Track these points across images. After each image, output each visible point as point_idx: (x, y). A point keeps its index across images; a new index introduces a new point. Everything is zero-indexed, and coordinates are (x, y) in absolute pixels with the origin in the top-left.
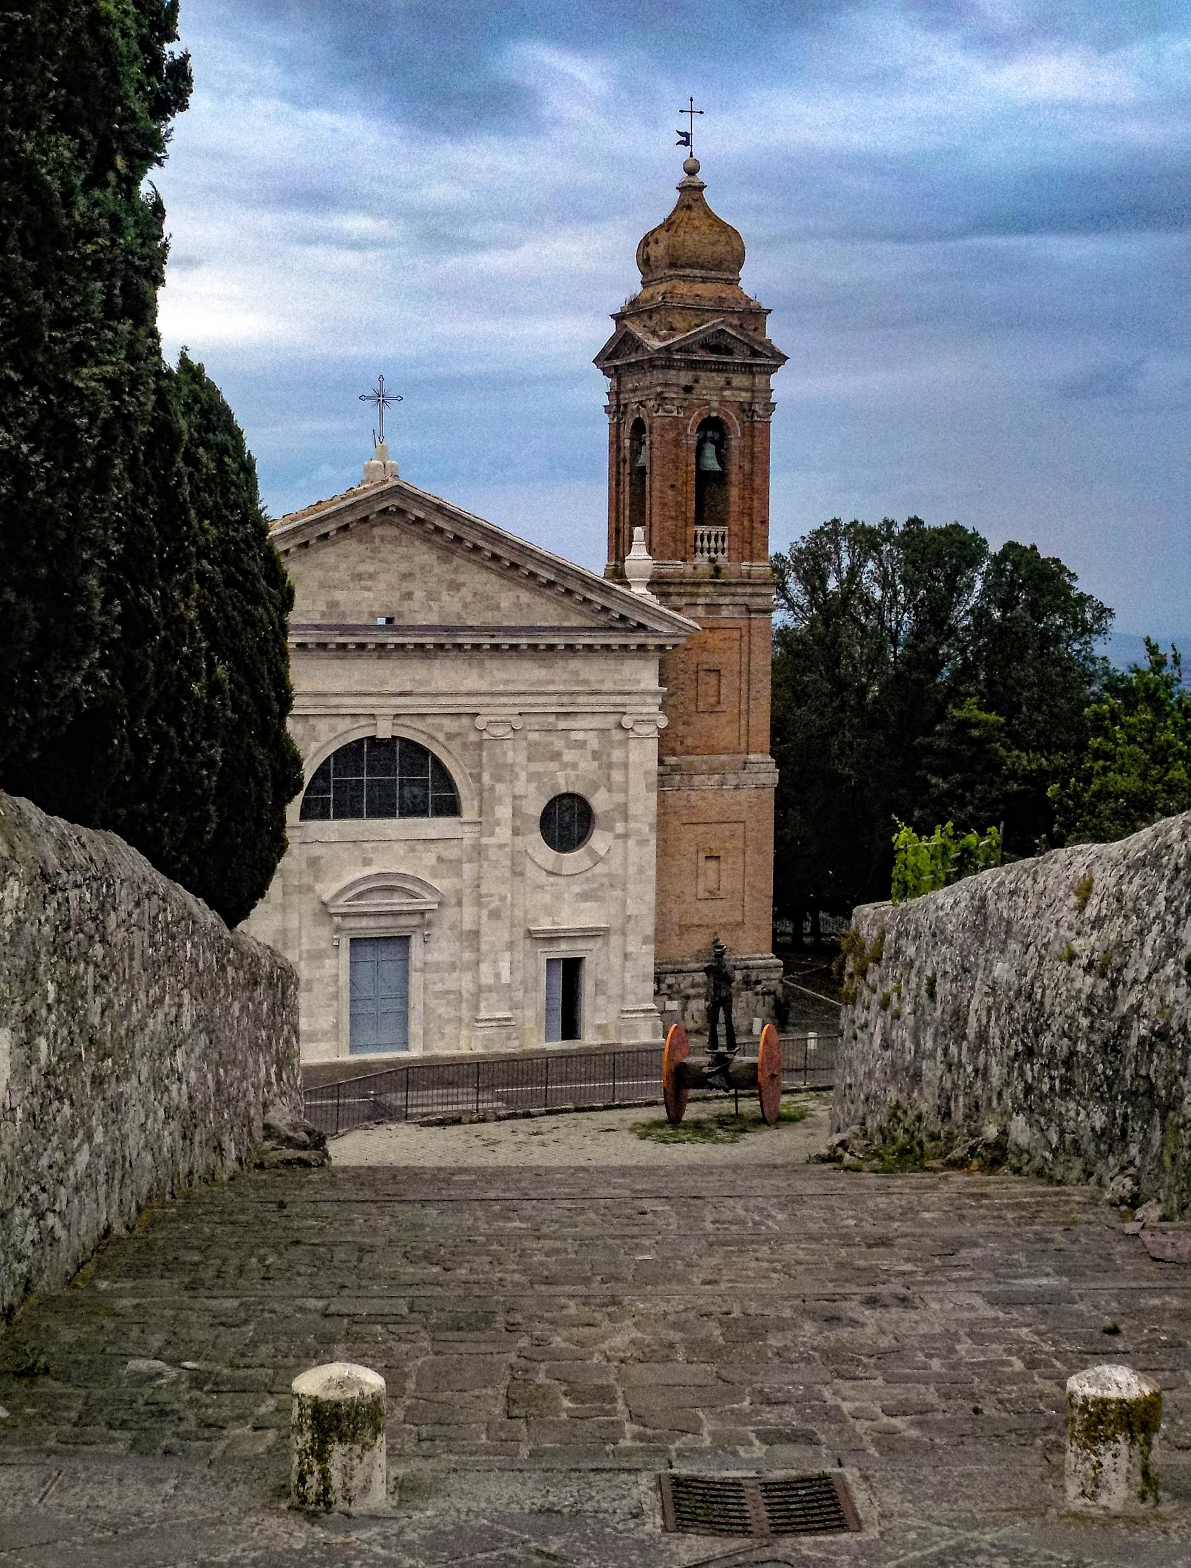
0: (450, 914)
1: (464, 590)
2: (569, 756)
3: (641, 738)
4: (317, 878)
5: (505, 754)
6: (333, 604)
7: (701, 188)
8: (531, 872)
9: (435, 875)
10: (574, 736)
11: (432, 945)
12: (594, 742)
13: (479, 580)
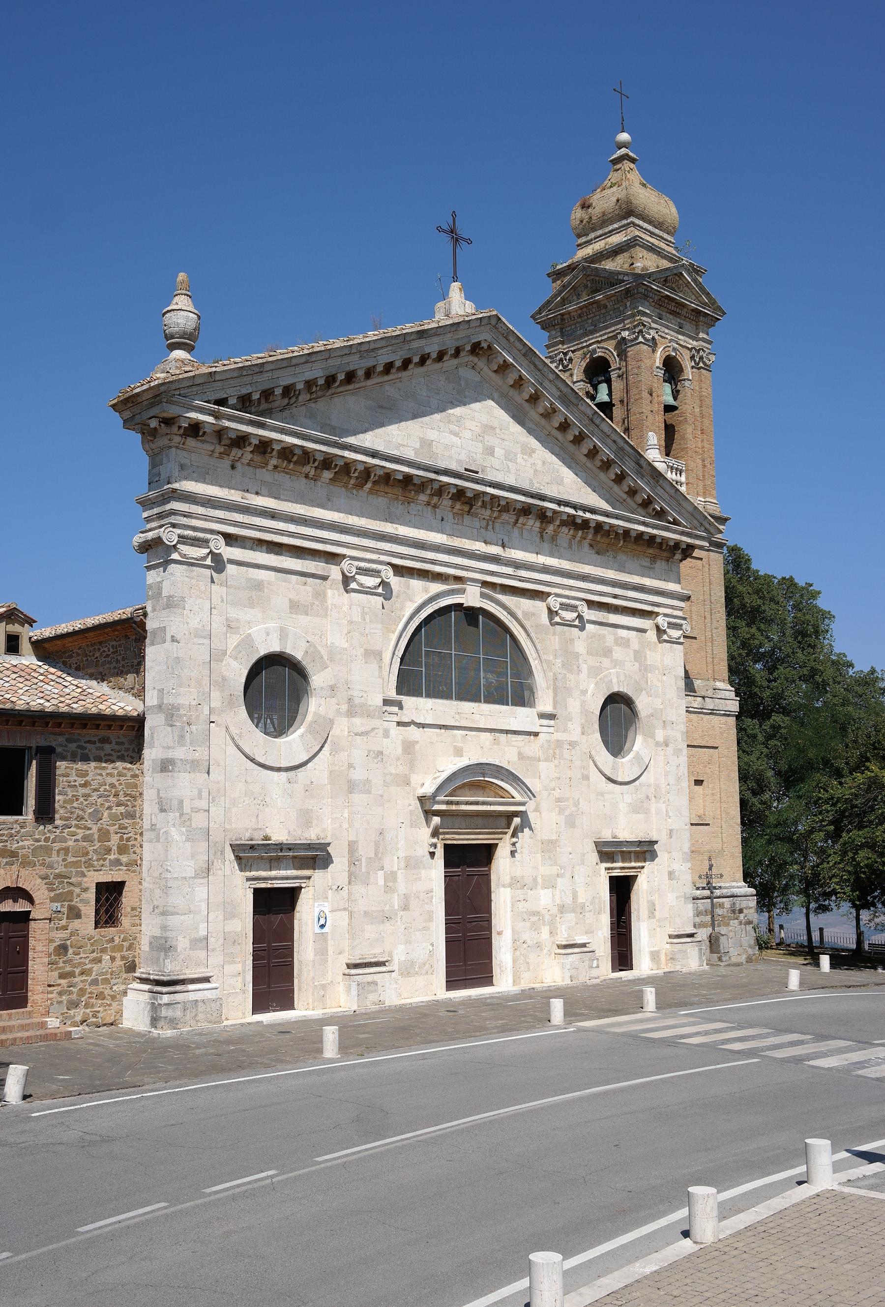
2: (618, 653)
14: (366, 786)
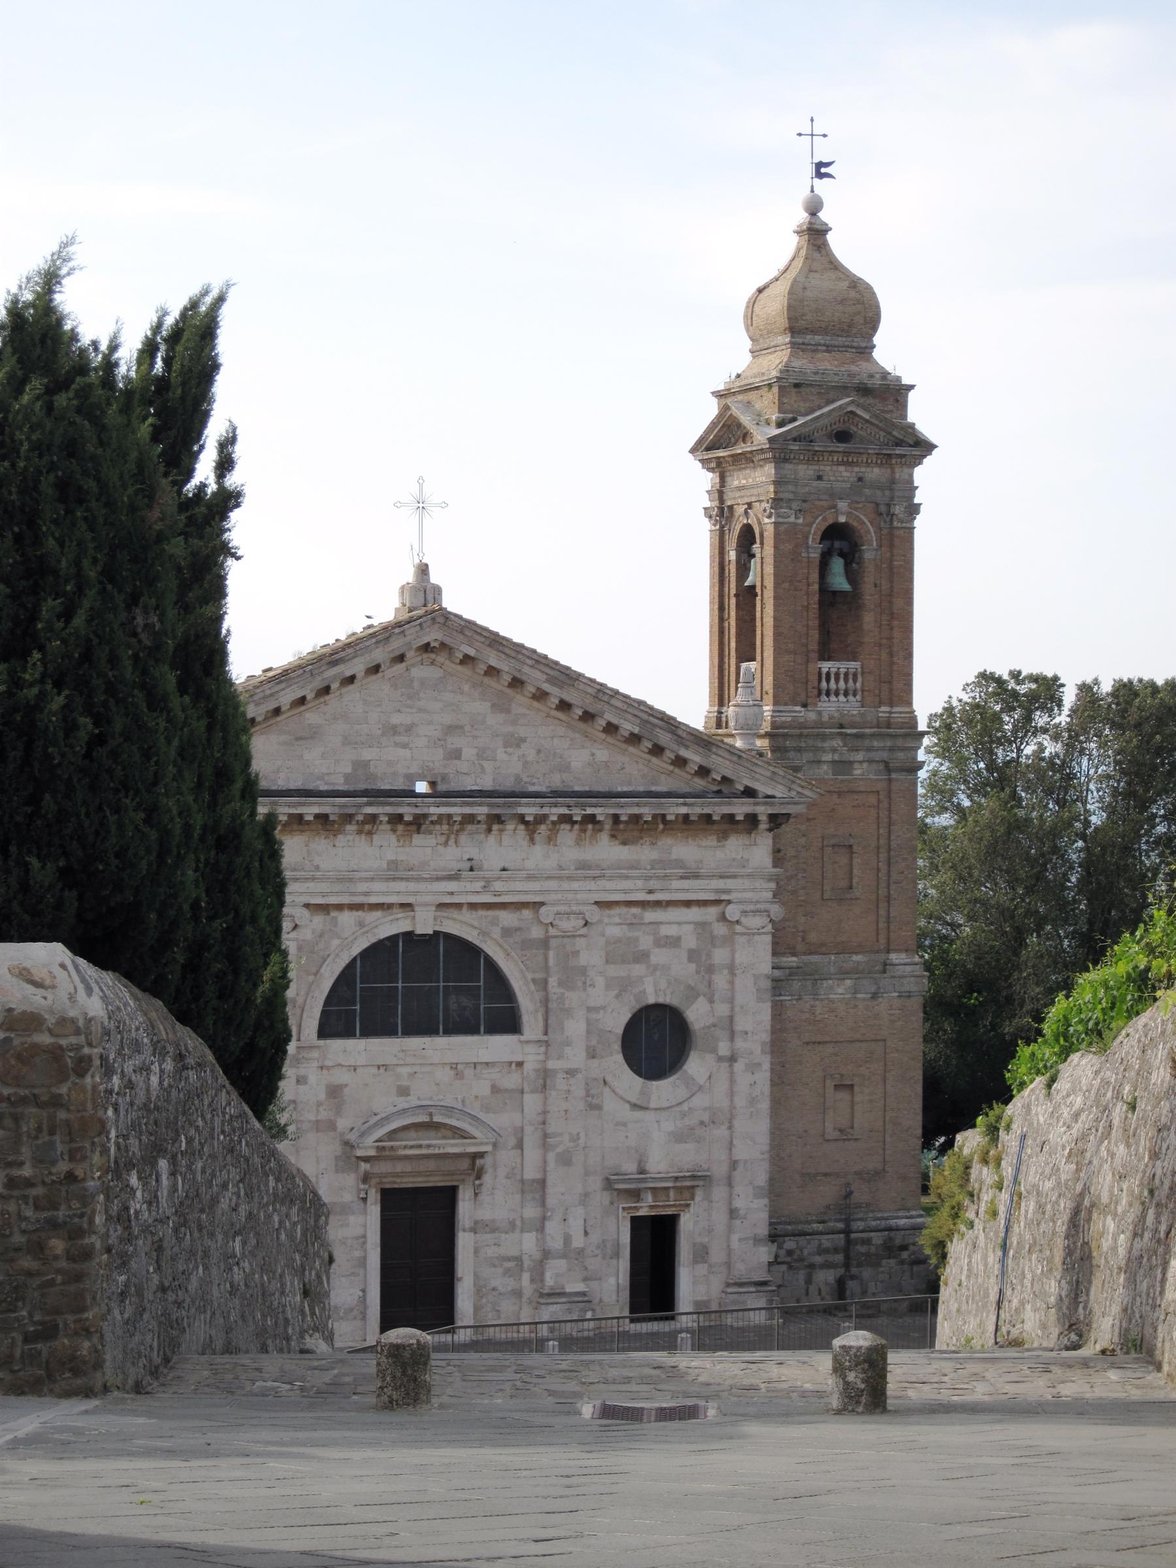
0: (506, 1157)
2: (659, 956)
3: (750, 934)
6: (361, 765)
8: (610, 1103)
9: (487, 1108)
11: (484, 1197)
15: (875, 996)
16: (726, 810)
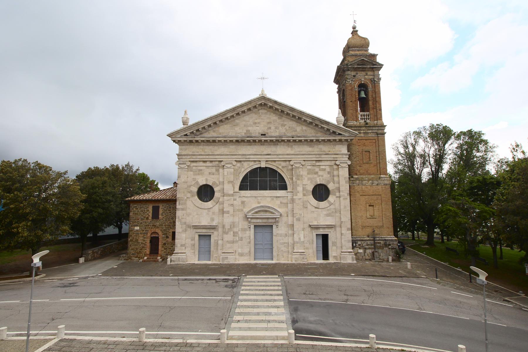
0: (284, 219)
1: (286, 126)
2: (320, 173)
3: (342, 167)
4: (244, 207)
5: (300, 172)
7: (357, 31)
8: (309, 207)
9: (279, 207)
10: (321, 167)
11: (279, 228)
12: (328, 169)
13: (290, 124)
14: (228, 212)
15: (377, 185)
16: (334, 138)
